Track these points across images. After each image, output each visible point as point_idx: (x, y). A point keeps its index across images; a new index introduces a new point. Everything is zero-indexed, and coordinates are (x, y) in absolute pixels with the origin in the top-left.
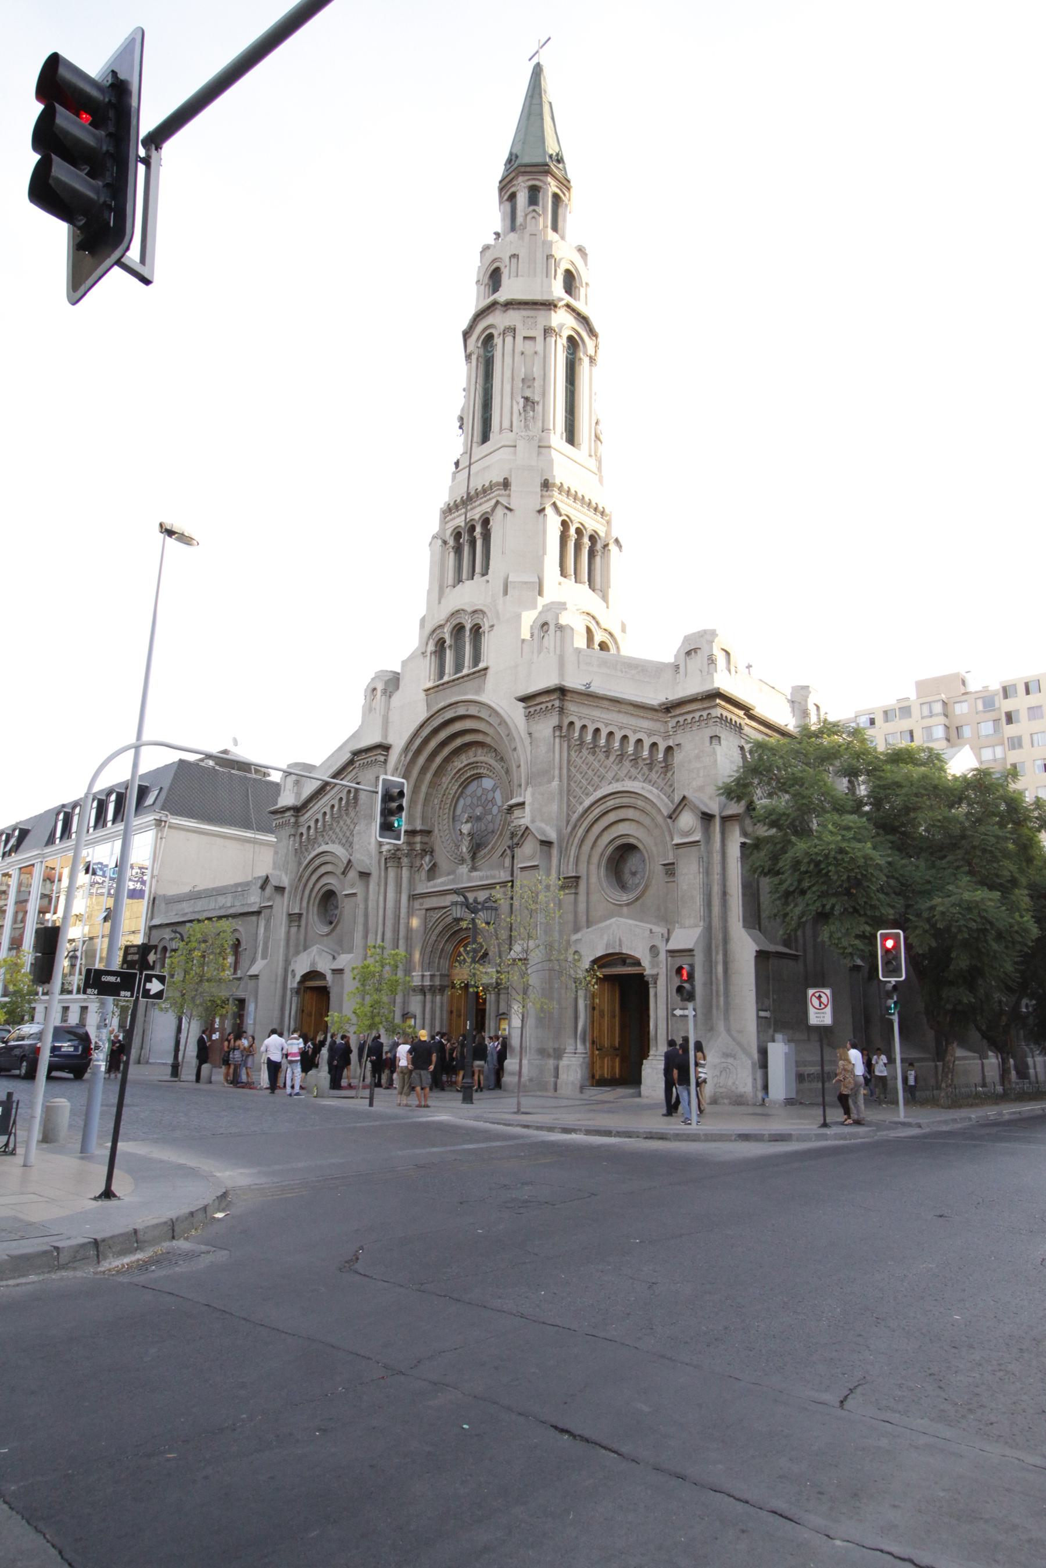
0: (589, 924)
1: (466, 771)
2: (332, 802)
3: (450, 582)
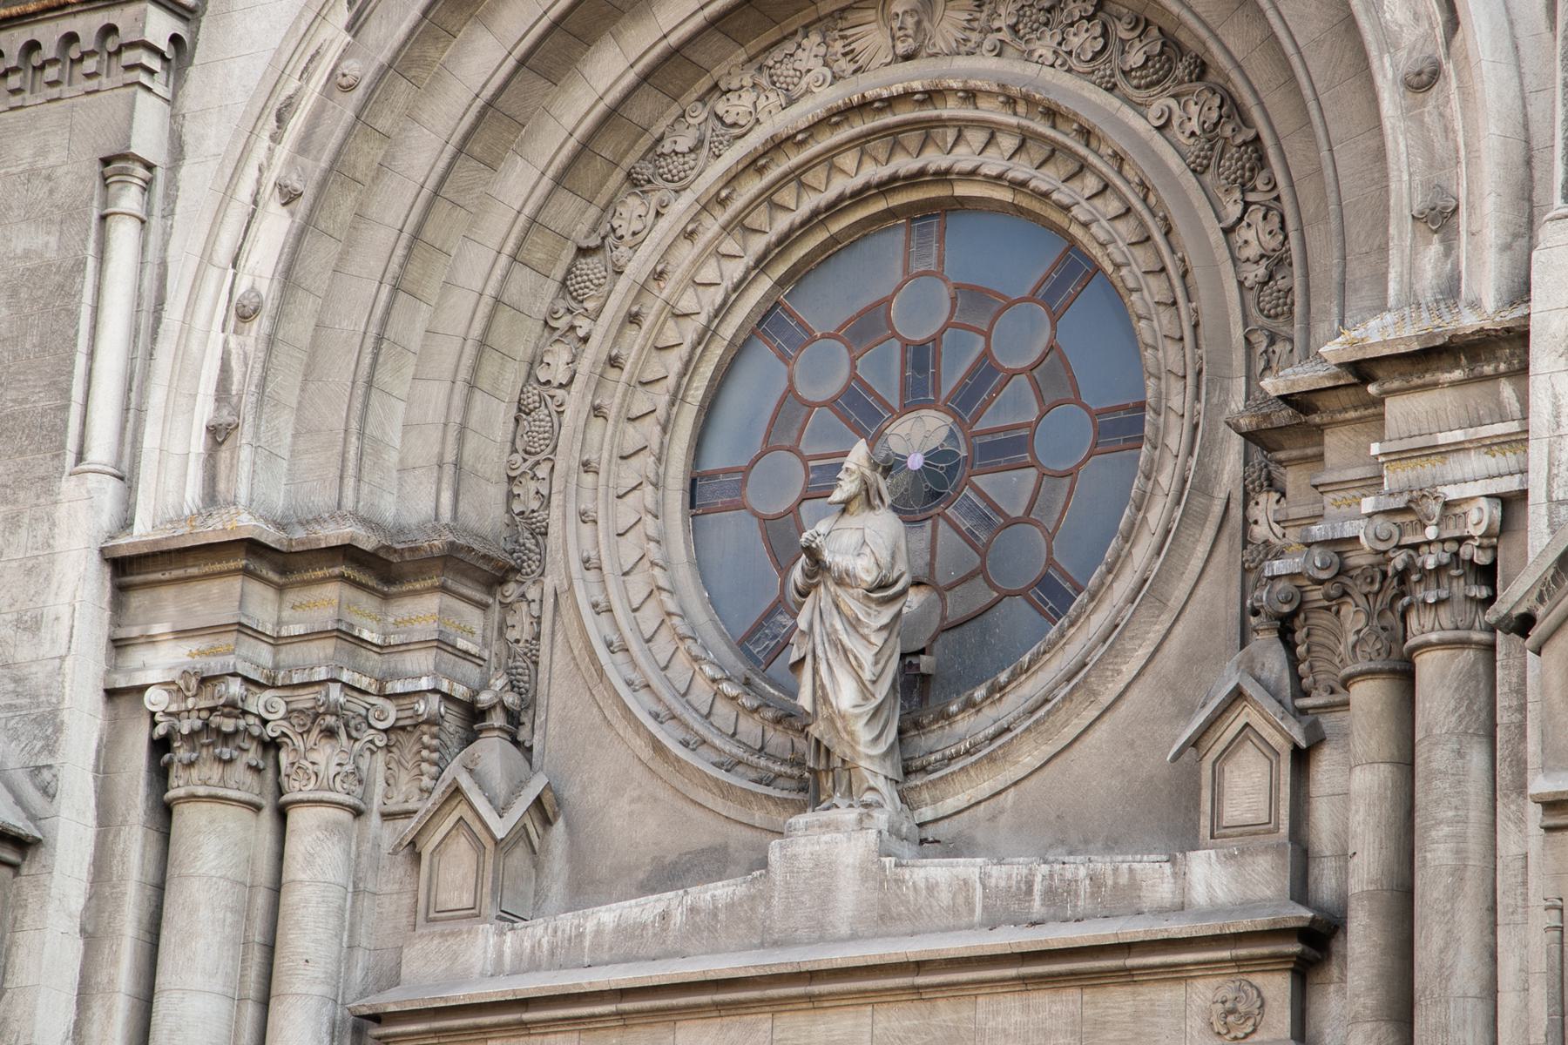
1: (828, 158)
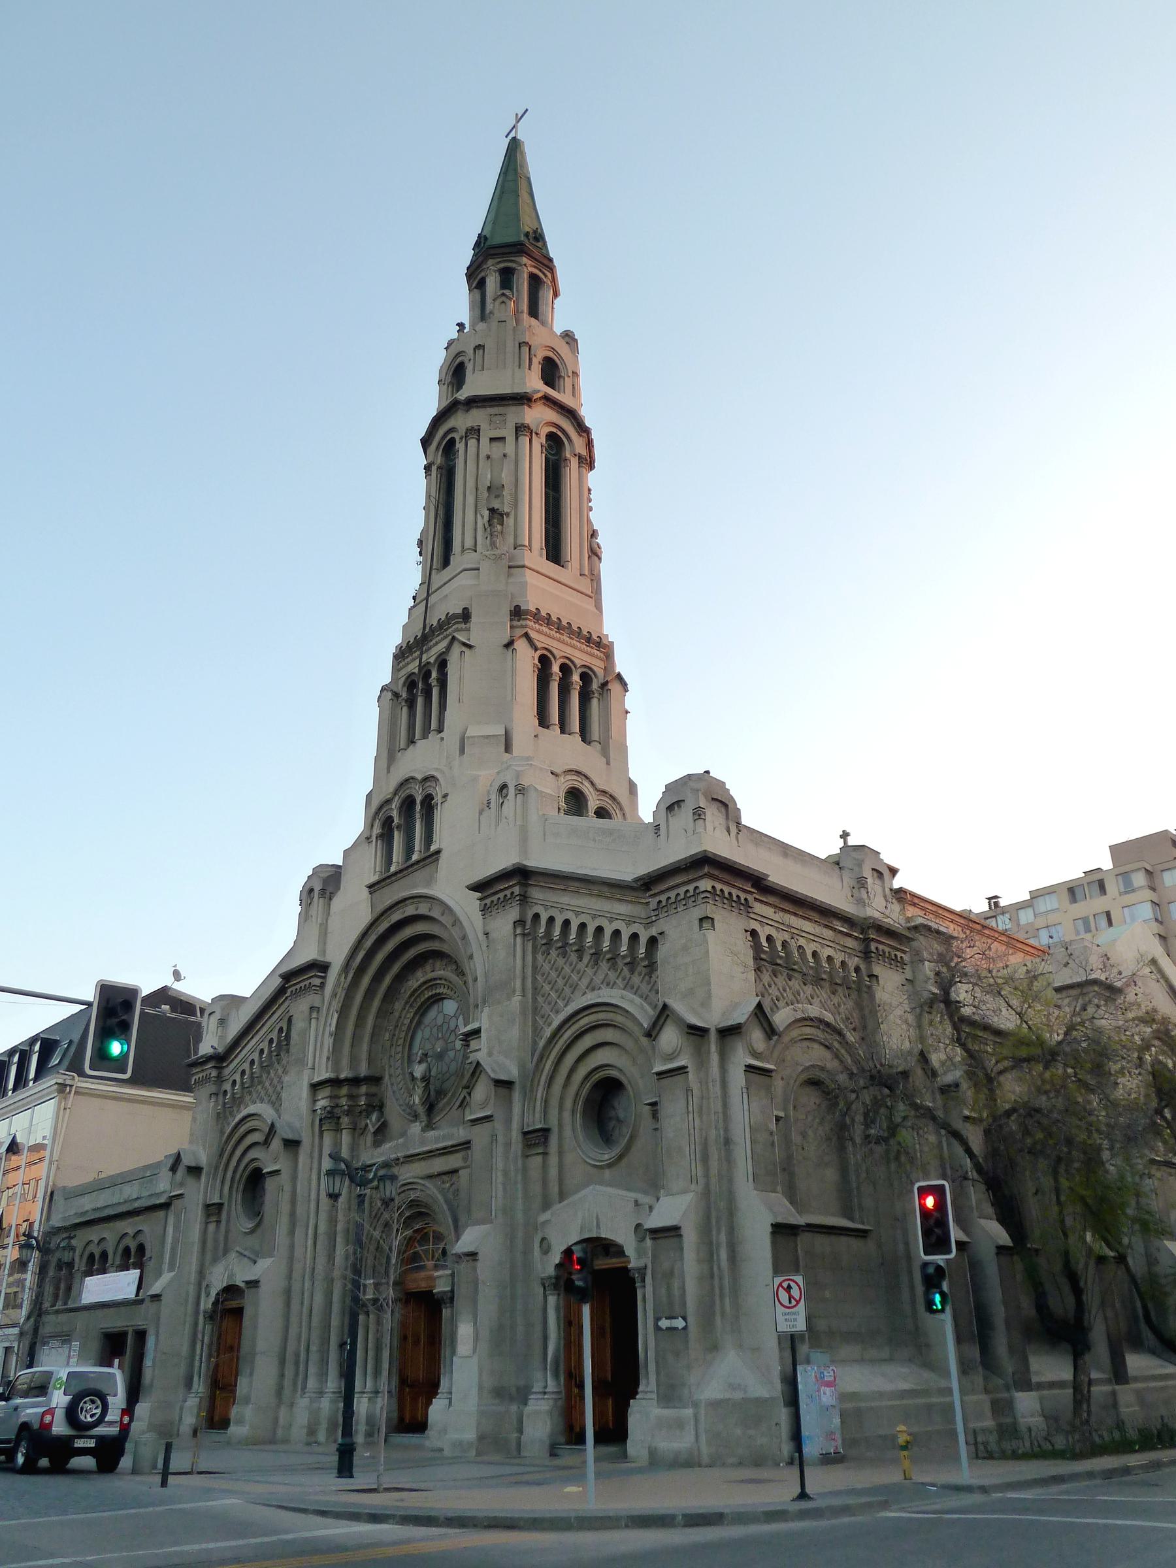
0: (562, 1196)
1: (422, 991)
2: (261, 1046)
3: (403, 745)
